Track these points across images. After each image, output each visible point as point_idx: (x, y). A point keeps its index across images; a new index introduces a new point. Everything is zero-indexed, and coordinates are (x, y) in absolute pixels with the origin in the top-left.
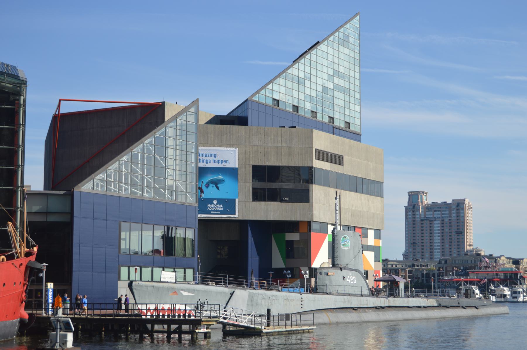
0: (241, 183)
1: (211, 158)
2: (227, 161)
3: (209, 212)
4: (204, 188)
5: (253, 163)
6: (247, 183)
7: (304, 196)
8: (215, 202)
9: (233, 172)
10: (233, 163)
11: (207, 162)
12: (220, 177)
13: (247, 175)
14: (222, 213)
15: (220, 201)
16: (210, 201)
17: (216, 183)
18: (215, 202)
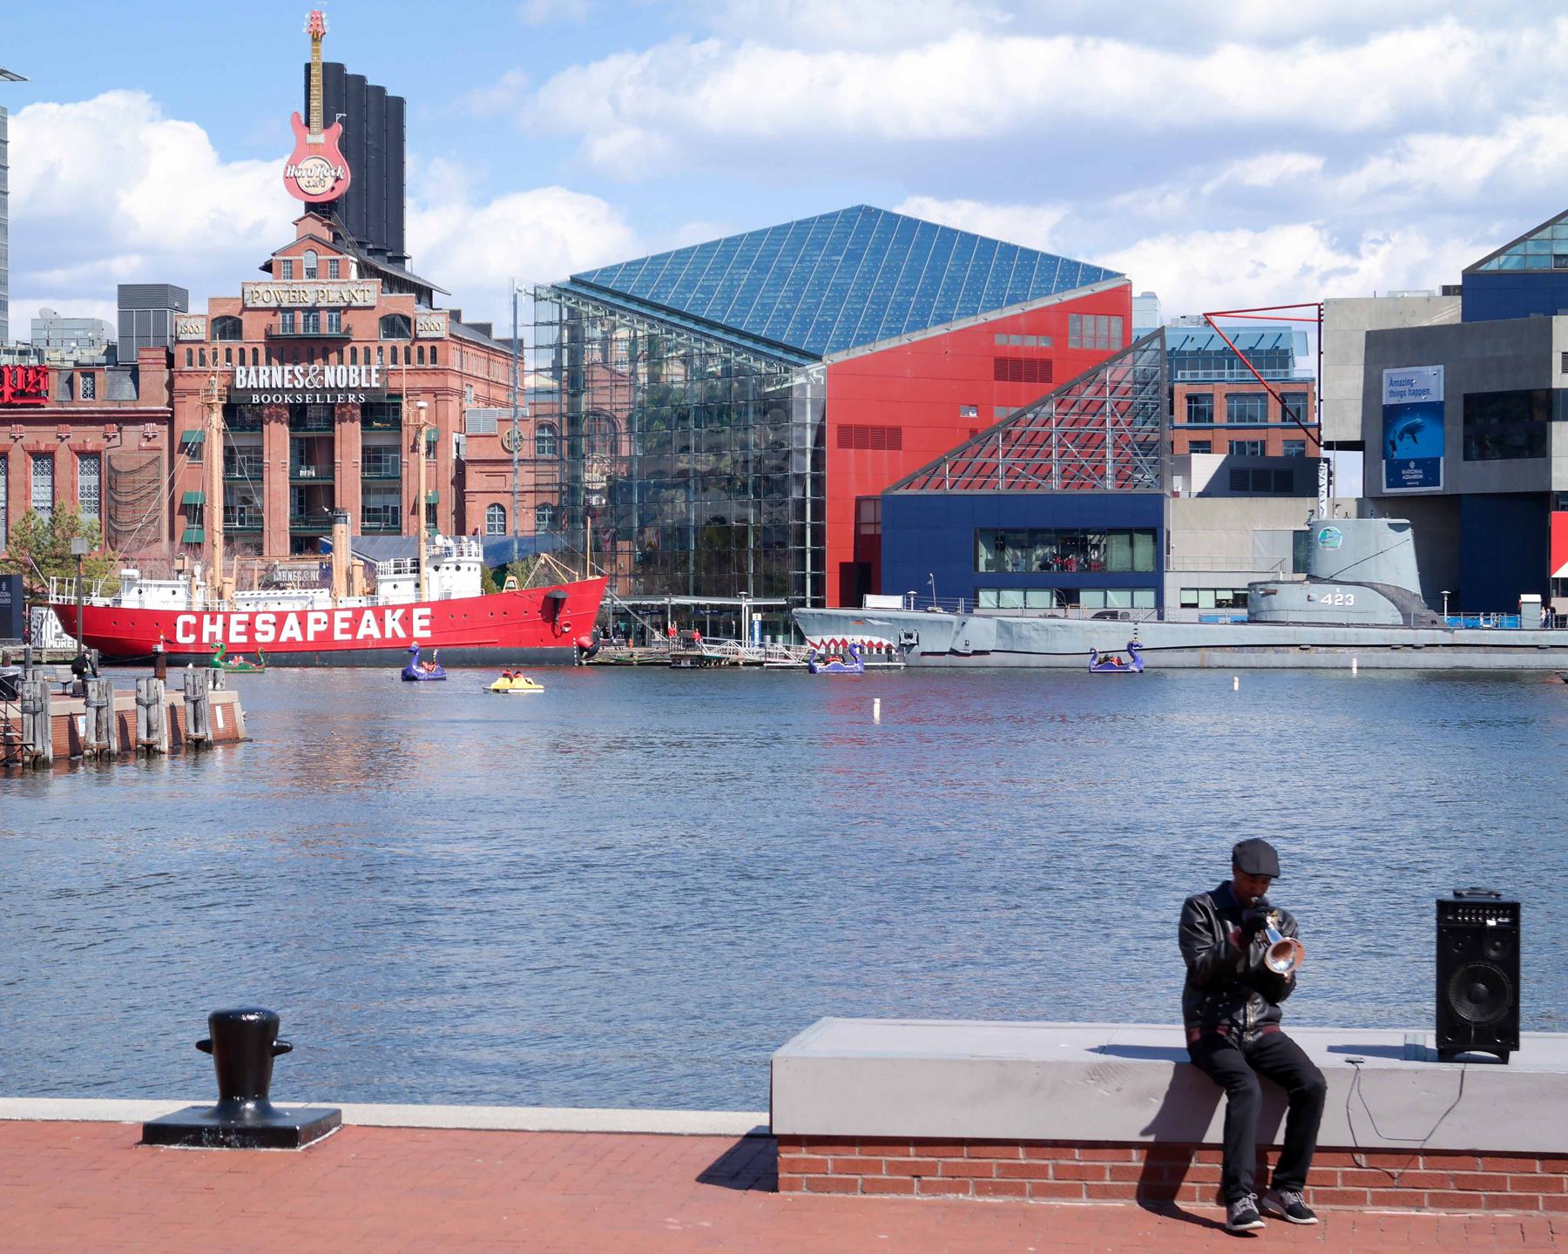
0: (1448, 428)
1: (1406, 388)
2: (1426, 391)
3: (1404, 484)
4: (1397, 442)
5: (1464, 391)
6: (1455, 428)
7: (1537, 447)
8: (1412, 465)
9: (1434, 410)
10: (1437, 395)
11: (1402, 394)
12: (1419, 420)
13: (1455, 413)
14: (1422, 483)
15: (1420, 463)
16: (1404, 464)
17: (1412, 431)
18: (1412, 465)
